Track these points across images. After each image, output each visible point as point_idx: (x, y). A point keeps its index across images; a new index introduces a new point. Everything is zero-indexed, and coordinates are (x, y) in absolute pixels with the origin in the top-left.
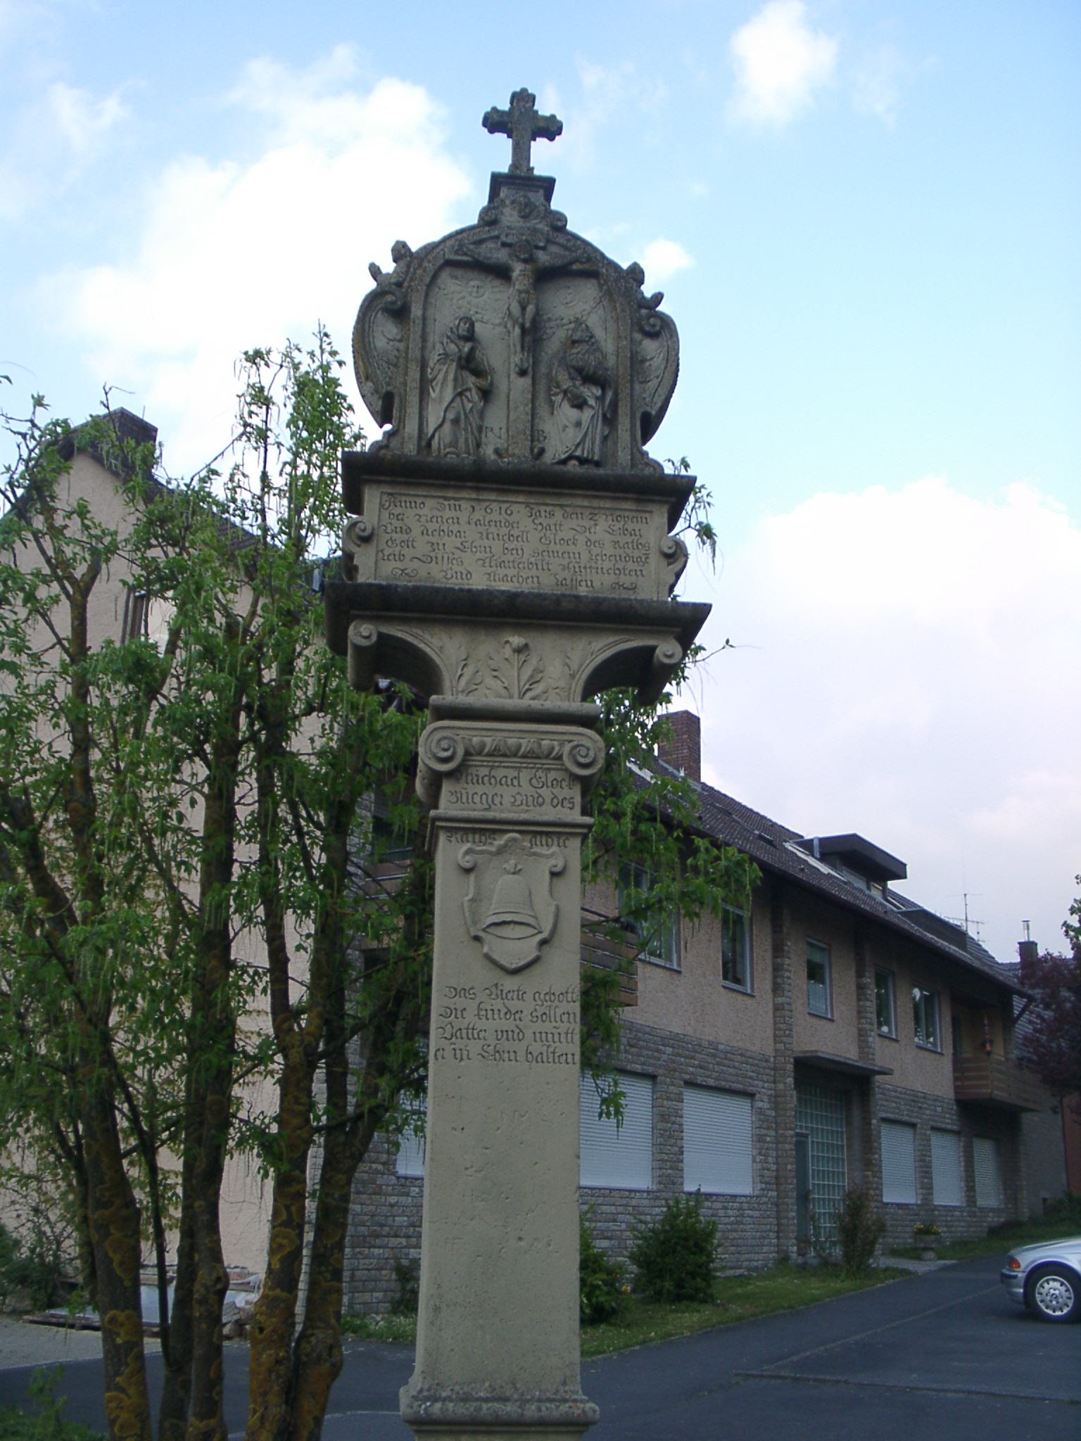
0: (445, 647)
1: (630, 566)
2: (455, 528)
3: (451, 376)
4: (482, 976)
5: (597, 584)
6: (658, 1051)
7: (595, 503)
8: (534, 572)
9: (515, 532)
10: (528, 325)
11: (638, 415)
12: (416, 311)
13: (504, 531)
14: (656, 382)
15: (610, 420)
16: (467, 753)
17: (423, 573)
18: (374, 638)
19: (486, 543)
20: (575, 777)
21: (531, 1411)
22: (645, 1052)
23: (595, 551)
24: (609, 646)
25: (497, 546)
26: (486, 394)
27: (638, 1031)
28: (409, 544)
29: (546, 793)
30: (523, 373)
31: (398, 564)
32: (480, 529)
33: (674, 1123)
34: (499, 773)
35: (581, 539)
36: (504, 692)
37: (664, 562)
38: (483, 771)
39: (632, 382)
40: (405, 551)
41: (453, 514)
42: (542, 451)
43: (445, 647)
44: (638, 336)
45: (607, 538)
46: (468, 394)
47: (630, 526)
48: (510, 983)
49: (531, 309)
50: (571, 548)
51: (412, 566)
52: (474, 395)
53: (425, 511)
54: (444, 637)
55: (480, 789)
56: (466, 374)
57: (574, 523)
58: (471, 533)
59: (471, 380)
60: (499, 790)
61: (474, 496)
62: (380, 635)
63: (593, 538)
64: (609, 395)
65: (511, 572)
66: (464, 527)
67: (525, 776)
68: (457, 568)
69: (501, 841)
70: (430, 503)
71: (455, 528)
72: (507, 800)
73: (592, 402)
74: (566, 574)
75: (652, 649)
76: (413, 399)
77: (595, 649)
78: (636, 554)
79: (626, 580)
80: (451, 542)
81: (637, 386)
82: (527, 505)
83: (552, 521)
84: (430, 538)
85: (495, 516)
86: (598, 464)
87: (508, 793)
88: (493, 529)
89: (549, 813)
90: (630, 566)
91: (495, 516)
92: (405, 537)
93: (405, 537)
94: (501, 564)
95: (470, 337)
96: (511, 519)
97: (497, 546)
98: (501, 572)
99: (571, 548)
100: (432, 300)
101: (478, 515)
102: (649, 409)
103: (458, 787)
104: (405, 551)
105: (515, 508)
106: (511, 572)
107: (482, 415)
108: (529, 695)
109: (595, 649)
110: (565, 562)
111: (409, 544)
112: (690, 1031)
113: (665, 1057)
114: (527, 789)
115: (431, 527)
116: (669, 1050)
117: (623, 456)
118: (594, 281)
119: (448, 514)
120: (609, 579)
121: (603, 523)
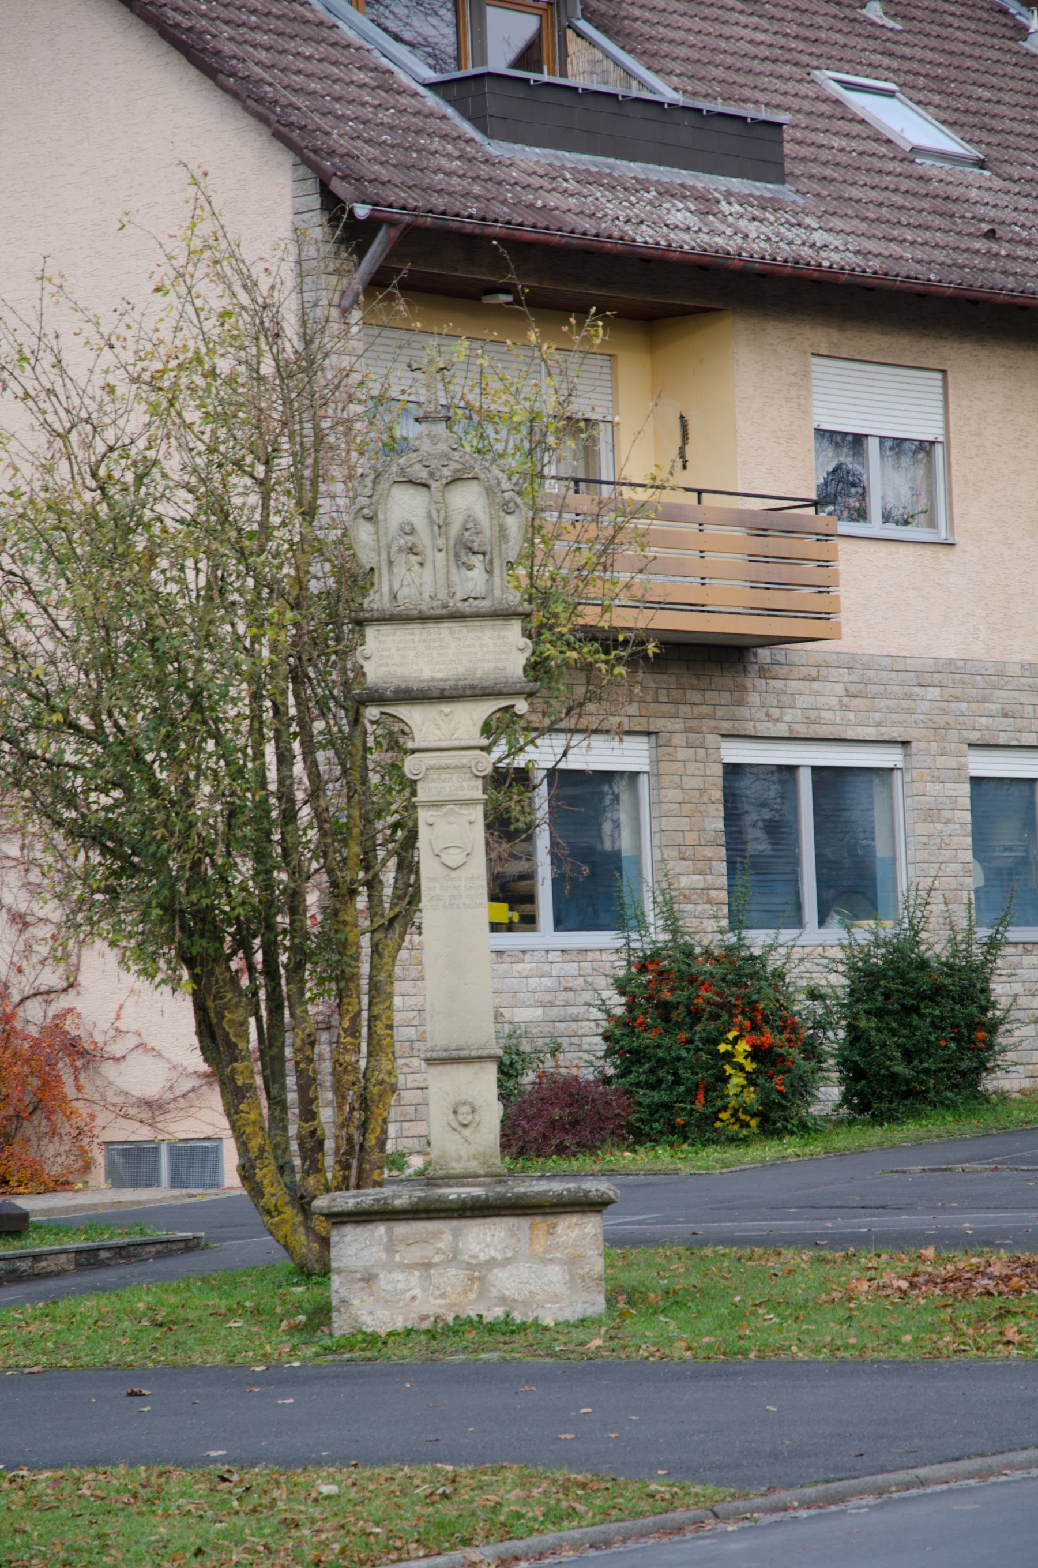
1: (503, 656)
4: (442, 871)
6: (909, 697)
12: (381, 516)
15: (489, 572)
20: (477, 777)
21: (474, 1054)
22: (882, 703)
23: (485, 650)
26: (421, 564)
27: (867, 667)
28: (390, 657)
29: (465, 784)
30: (440, 550)
33: (948, 822)
34: (443, 776)
43: (413, 716)
44: (502, 514)
48: (454, 874)
49: (442, 512)
52: (417, 567)
53: (397, 638)
55: (434, 785)
56: (411, 556)
59: (413, 559)
67: (455, 777)
69: (445, 809)
70: (399, 632)
73: (478, 565)
77: (485, 709)
79: (501, 665)
80: (412, 653)
81: (504, 546)
85: (432, 636)
87: (447, 786)
89: (468, 794)
91: (432, 636)
94: (437, 663)
107: (421, 576)
109: (485, 709)
111: (390, 657)
112: (978, 651)
113: (924, 706)
115: (401, 645)
116: (934, 693)
117: (497, 592)
119: (409, 637)
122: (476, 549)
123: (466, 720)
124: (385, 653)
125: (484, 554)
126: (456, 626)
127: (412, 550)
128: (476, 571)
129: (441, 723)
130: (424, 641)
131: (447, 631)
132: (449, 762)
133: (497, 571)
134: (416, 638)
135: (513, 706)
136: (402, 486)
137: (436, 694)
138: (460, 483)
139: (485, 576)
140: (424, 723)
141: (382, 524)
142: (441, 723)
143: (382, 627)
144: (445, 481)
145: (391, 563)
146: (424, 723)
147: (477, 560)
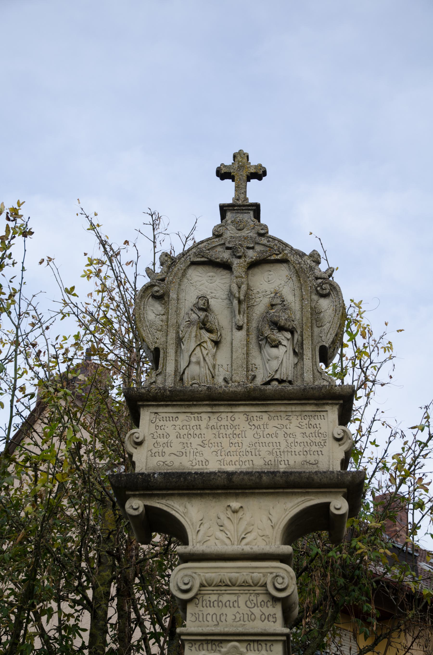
0: (189, 512)
1: (314, 448)
2: (198, 432)
3: (193, 334)
5: (292, 463)
7: (289, 408)
8: (250, 457)
9: (237, 432)
10: (242, 298)
11: (317, 349)
12: (173, 295)
13: (229, 431)
14: (328, 325)
15: (298, 354)
16: (202, 585)
17: (177, 464)
18: (141, 509)
19: (218, 440)
20: (275, 599)
24: (298, 504)
25: (225, 442)
26: (217, 343)
28: (168, 444)
29: (257, 611)
30: (240, 328)
31: (162, 459)
32: (214, 431)
34: (225, 598)
35: (281, 433)
36: (227, 541)
37: (336, 444)
38: (214, 598)
39: (312, 327)
40: (166, 450)
41: (197, 423)
42: (254, 377)
43: (189, 512)
44: (315, 297)
45: (298, 431)
46: (205, 345)
47: (313, 422)
49: (244, 287)
50: (275, 440)
51: (168, 459)
52: (210, 345)
53: (178, 422)
54: (189, 505)
55: (211, 611)
56: (203, 332)
57: (275, 423)
58: (209, 434)
59: (206, 335)
60: (225, 610)
61: (209, 410)
62: (146, 507)
63: (288, 431)
64: (296, 336)
65: (234, 458)
66: (204, 431)
67: (242, 599)
68: (199, 458)
69: (226, 648)
70: (182, 417)
71: (198, 432)
72: (230, 618)
73: (285, 342)
74: (271, 458)
75: (328, 505)
76: (171, 351)
77: (290, 507)
78: (318, 440)
79: (311, 458)
80: (196, 441)
81: (316, 330)
82: (245, 413)
83: (261, 423)
84: (182, 440)
85: (224, 422)
86: (290, 382)
87: (230, 612)
88: (222, 431)
89: (258, 626)
90: (314, 448)
91: (224, 422)
92: (165, 440)
93: (165, 440)
95: (206, 309)
96: (235, 423)
97: (225, 442)
98: (228, 459)
99: (275, 440)
100: (183, 287)
101: (213, 422)
102: (324, 344)
103: (197, 610)
104: (166, 450)
105: (236, 416)
106: (234, 458)
107: (214, 356)
108: (244, 541)
109: (290, 507)
110: (270, 449)
111: (168, 444)
114: (244, 609)
115: (182, 432)
117: (308, 377)
118: (285, 265)
120: (299, 459)
121: (295, 421)
122: (282, 323)
123: (263, 523)
124: (161, 441)
125: (292, 332)
126: (254, 411)
127: (204, 325)
128: (282, 349)
129: (227, 523)
130: (213, 428)
131: (243, 417)
132: (234, 575)
133: (308, 354)
134: (203, 424)
135: (328, 505)
136: (200, 269)
137: (220, 481)
138: (267, 267)
139: (292, 359)
140: (205, 523)
141: (173, 303)
142: (227, 523)
143: (160, 410)
144: (248, 260)
145: (179, 341)
146: (205, 523)
147: (283, 337)
